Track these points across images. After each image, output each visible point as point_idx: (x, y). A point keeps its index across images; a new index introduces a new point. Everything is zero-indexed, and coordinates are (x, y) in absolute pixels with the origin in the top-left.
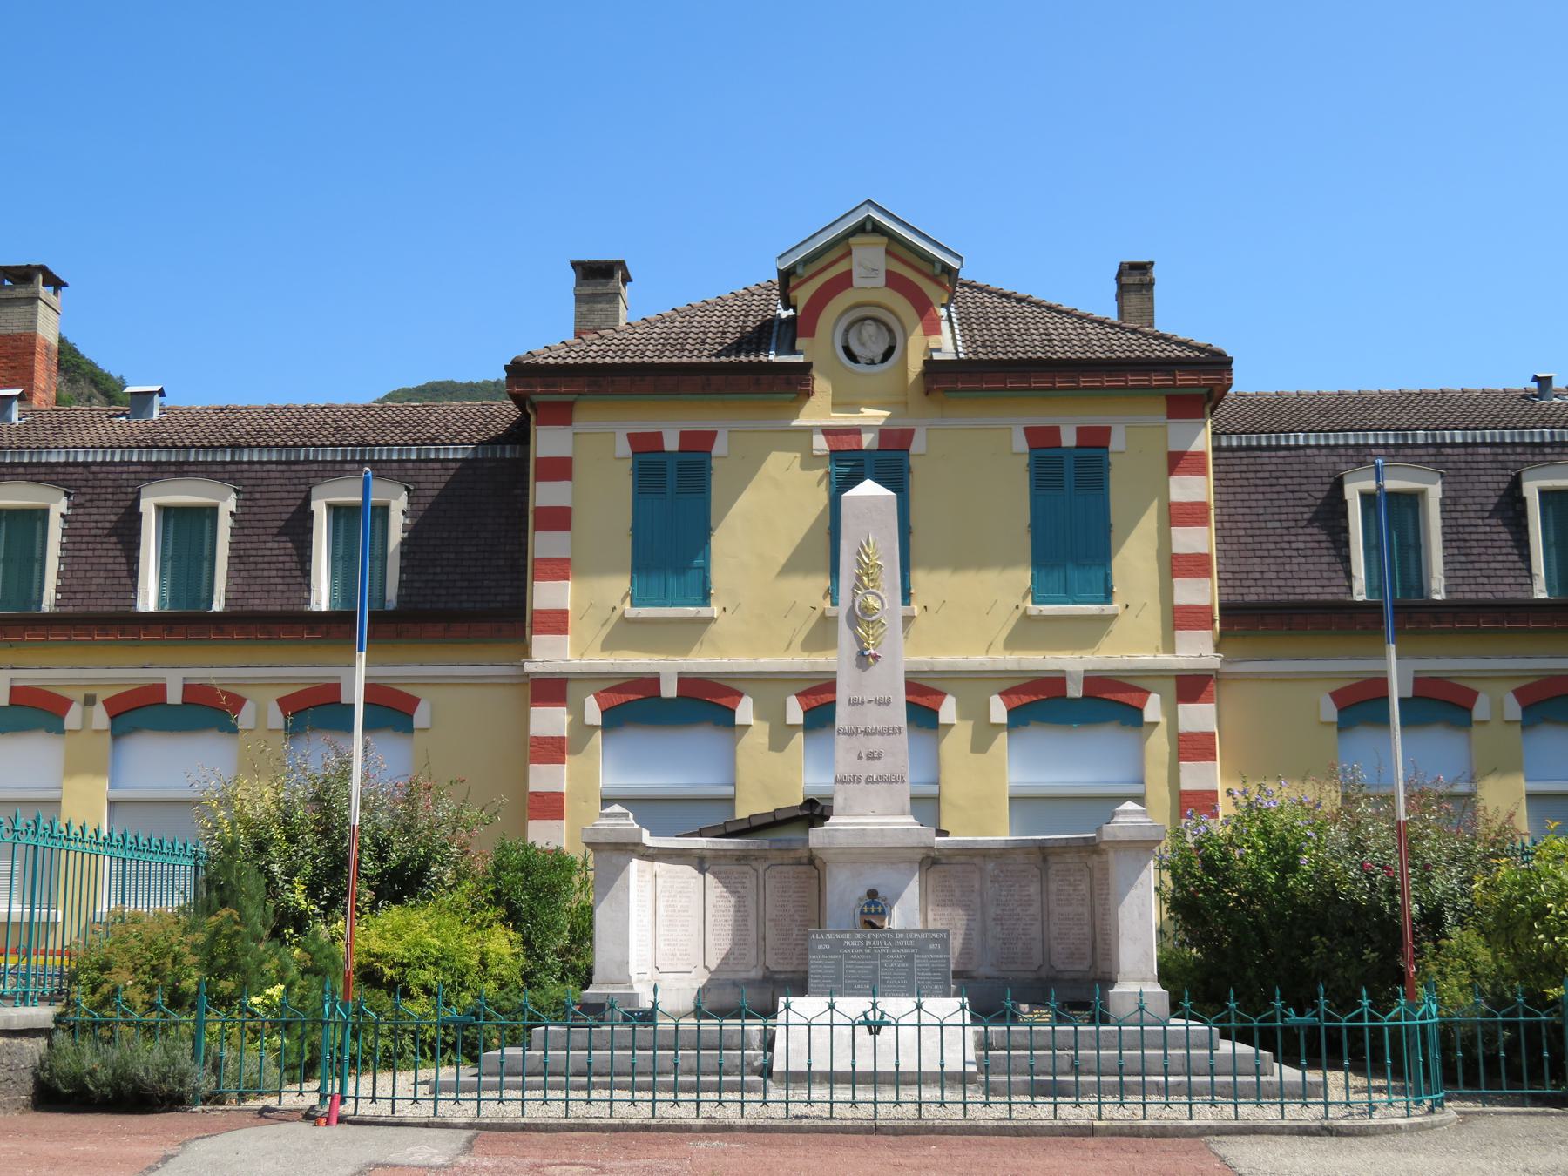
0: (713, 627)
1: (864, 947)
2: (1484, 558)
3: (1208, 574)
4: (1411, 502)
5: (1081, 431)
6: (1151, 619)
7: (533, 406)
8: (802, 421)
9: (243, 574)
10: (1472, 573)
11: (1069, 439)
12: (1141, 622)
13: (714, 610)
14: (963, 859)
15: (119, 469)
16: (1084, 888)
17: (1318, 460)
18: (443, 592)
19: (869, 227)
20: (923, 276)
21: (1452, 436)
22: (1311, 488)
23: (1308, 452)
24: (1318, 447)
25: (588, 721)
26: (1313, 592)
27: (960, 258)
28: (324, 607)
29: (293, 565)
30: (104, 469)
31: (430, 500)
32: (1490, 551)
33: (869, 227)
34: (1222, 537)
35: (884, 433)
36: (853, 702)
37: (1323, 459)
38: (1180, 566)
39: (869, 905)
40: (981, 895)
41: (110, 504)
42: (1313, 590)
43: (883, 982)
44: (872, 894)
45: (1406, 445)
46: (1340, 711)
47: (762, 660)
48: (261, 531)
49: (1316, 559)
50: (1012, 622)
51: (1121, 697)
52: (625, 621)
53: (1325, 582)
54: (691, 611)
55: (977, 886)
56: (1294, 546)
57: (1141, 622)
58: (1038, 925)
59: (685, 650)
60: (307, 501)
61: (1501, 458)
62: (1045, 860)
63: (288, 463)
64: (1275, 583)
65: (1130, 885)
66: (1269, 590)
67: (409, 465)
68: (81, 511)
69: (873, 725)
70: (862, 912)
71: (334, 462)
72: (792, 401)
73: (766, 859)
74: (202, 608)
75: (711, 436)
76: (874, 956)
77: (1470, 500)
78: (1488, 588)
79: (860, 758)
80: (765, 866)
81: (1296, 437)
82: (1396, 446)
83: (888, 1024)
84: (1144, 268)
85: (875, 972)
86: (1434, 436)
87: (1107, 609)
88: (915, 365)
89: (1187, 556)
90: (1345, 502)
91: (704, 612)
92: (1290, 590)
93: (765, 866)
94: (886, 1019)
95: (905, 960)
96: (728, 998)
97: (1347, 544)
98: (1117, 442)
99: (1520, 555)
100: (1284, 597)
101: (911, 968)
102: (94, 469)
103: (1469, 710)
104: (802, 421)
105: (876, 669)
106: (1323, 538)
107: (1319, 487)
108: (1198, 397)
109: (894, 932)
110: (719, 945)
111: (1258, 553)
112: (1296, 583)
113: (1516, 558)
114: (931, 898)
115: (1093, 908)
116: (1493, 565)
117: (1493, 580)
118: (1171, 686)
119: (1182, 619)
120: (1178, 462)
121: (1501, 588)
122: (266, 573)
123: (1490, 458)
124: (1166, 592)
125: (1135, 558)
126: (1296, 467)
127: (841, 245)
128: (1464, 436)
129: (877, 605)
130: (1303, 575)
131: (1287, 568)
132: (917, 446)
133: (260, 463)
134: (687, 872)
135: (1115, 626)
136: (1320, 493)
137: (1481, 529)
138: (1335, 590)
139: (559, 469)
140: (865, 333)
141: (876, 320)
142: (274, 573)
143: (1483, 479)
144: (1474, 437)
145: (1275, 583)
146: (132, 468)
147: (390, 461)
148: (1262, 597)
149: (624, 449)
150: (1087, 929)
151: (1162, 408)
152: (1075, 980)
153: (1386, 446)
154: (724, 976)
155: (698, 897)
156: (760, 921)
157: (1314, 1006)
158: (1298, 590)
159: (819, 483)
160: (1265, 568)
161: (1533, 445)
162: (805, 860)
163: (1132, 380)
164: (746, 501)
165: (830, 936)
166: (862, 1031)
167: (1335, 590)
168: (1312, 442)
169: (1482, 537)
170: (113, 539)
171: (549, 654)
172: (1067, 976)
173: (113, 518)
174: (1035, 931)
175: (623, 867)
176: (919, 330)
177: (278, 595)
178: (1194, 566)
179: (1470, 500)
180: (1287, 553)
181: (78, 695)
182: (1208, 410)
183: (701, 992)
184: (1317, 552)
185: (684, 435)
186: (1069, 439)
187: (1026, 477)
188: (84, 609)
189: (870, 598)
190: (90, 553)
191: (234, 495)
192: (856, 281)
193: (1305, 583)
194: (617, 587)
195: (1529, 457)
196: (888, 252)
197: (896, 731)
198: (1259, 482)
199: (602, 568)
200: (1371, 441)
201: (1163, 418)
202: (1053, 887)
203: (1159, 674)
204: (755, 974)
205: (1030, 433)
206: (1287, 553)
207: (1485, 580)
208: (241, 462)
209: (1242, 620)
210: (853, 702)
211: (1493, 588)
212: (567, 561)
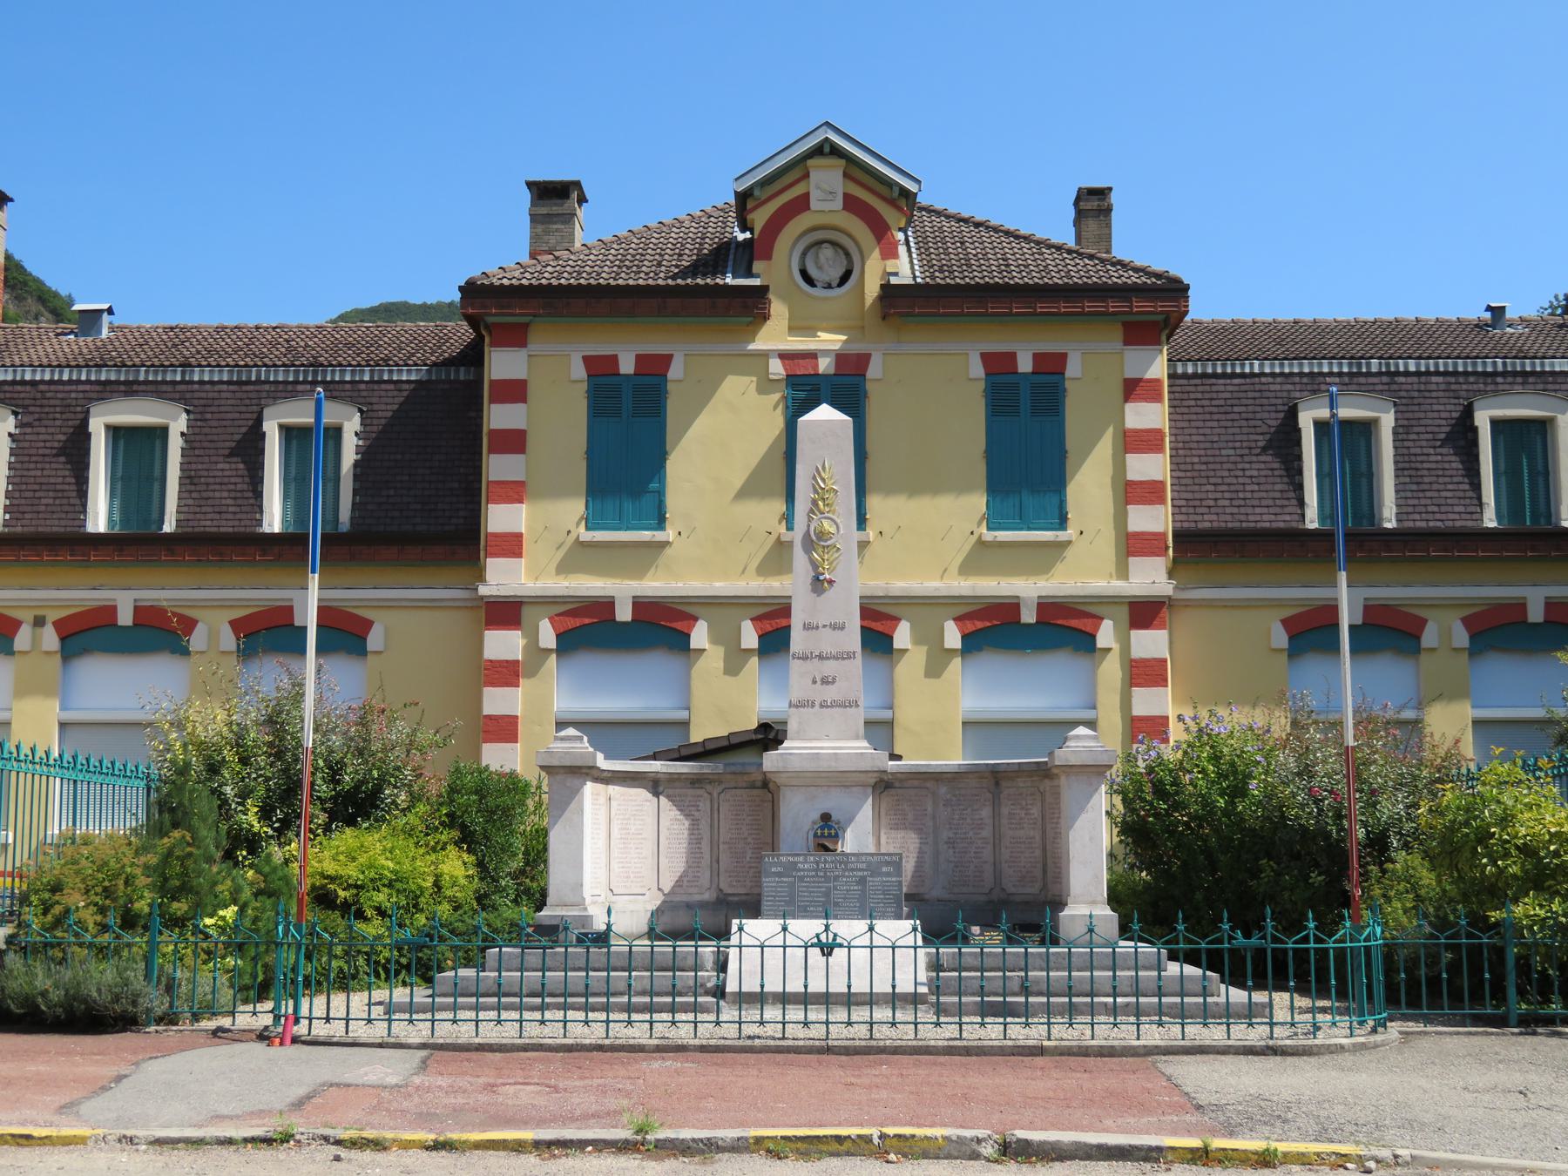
0: (668, 551)
1: (816, 870)
2: (1435, 487)
3: (1162, 501)
4: (1366, 429)
5: (1038, 358)
6: (1105, 545)
7: (487, 327)
8: (758, 345)
9: (194, 495)
10: (1423, 502)
11: (1025, 364)
12: (1091, 551)
13: (669, 534)
14: (916, 783)
15: (67, 388)
16: (1035, 812)
17: (1272, 387)
18: (397, 514)
19: (827, 149)
20: (881, 200)
21: (1406, 365)
22: (1266, 415)
23: (1263, 380)
24: (1273, 375)
25: (542, 645)
26: (1265, 519)
27: (918, 182)
28: (277, 529)
29: (245, 487)
30: (53, 388)
31: (383, 421)
32: (1441, 480)
33: (827, 149)
34: (1176, 465)
35: (841, 358)
36: (808, 627)
37: (1278, 387)
38: (1135, 493)
39: (822, 828)
40: (934, 818)
41: (58, 423)
42: (1265, 517)
43: (837, 904)
44: (826, 817)
45: (1359, 374)
46: (1291, 638)
47: (717, 584)
48: (212, 452)
49: (1269, 487)
50: (968, 547)
51: (1074, 623)
52: (579, 544)
53: (1278, 510)
54: (646, 535)
55: (930, 809)
56: (1248, 473)
57: (1091, 551)
58: (990, 847)
59: (640, 573)
60: (259, 421)
61: (1453, 387)
62: (997, 784)
63: (239, 383)
64: (1228, 510)
65: (1082, 809)
66: (1222, 518)
67: (363, 386)
68: (29, 430)
69: (828, 649)
70: (815, 835)
71: (286, 383)
73: (720, 782)
74: (153, 528)
75: (666, 360)
76: (827, 879)
77: (1422, 429)
78: (1438, 516)
79: (814, 682)
80: (720, 789)
81: (1252, 365)
82: (1350, 374)
83: (841, 946)
84: (1102, 193)
85: (827, 894)
86: (1388, 365)
87: (1062, 536)
88: (872, 290)
89: (1141, 483)
90: (1299, 430)
91: (659, 536)
92: (1243, 518)
93: (720, 789)
94: (839, 940)
95: (858, 883)
96: (682, 920)
97: (1300, 472)
98: (1073, 369)
99: (1471, 484)
100: (1237, 525)
101: (864, 891)
102: (42, 387)
103: (1418, 638)
104: (758, 345)
105: (831, 594)
106: (1276, 466)
107: (1273, 415)
108: (1155, 323)
109: (847, 855)
110: (673, 867)
111: (1212, 480)
112: (1250, 510)
113: (1467, 487)
114: (884, 821)
115: (1044, 832)
116: (1444, 494)
117: (1443, 509)
118: (1124, 613)
119: (1135, 545)
120: (1134, 389)
121: (1451, 516)
122: (217, 494)
123: (1443, 387)
124: (1121, 518)
125: (1089, 485)
126: (1250, 395)
127: (798, 167)
128: (1418, 365)
129: (833, 530)
130: (1256, 503)
131: (1241, 495)
132: (874, 371)
133: (211, 382)
134: (641, 795)
135: (1069, 553)
137: (1433, 458)
138: (1288, 518)
139: (514, 391)
140: (822, 258)
141: (834, 244)
142: (225, 494)
143: (1435, 407)
144: (1427, 366)
145: (1228, 510)
146: (81, 388)
147: (343, 382)
148: (1215, 525)
149: (579, 371)
150: (1038, 853)
151: (1118, 334)
152: (1027, 903)
153: (1340, 374)
154: (677, 899)
155: (652, 820)
156: (714, 844)
157: (1262, 929)
158: (1251, 518)
159: (775, 408)
160: (1219, 495)
161: (1485, 374)
162: (759, 784)
163: (1088, 306)
164: (702, 425)
165: (783, 859)
166: (815, 952)
167: (1288, 518)
168: (1267, 370)
169: (1433, 466)
170: (62, 459)
171: (503, 578)
172: (1018, 899)
173: (63, 438)
174: (987, 853)
175: (576, 791)
176: (876, 253)
177: (230, 516)
178: (1148, 493)
179: (1422, 429)
180: (1241, 480)
181: (26, 616)
182: (1164, 338)
183: (656, 914)
184: (1270, 480)
185: (639, 358)
186: (1025, 364)
187: (983, 402)
188: (32, 529)
189: (826, 524)
190: (39, 473)
191: (184, 416)
192: (814, 205)
193: (1258, 510)
194: (572, 510)
195: (1482, 386)
196: (846, 175)
197: (850, 656)
198: (1215, 410)
199: (557, 491)
200: (1326, 370)
201: (1119, 345)
202: (1005, 811)
203: (1112, 601)
204: (707, 896)
205: (987, 358)
206: (1241, 480)
207: (1436, 509)
208: (192, 382)
209: (1194, 547)
210: (808, 627)
211: (1443, 517)
212: (522, 484)
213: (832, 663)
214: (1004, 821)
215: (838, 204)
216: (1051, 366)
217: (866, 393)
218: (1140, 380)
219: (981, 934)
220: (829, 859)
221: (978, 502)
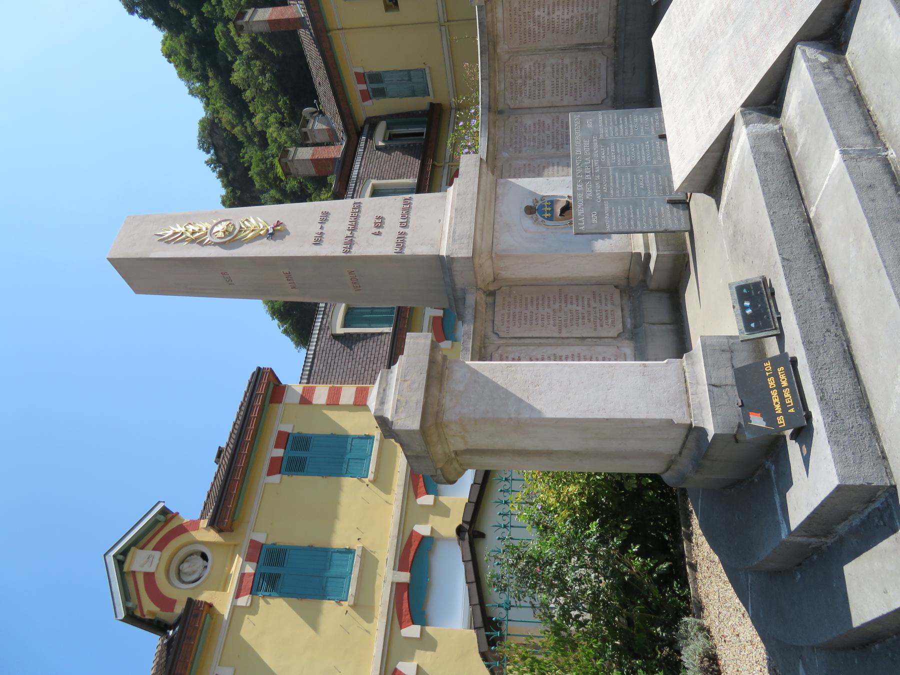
1: (593, 181)
19: (121, 557)
20: (162, 527)
24: (316, 346)
26: (386, 348)
27: (159, 502)
33: (121, 557)
35: (248, 559)
39: (542, 213)
44: (530, 210)
47: (375, 651)
50: (376, 489)
62: (501, 112)
70: (551, 219)
72: (212, 618)
73: (485, 337)
79: (379, 234)
80: (494, 337)
85: (622, 171)
88: (212, 536)
89: (356, 398)
97: (365, 334)
98: (287, 428)
120: (305, 400)
129: (224, 224)
132: (261, 538)
136: (338, 345)
151: (275, 405)
152: (616, 74)
153: (323, 318)
156: (562, 341)
159: (268, 603)
172: (611, 86)
176: (194, 533)
186: (280, 453)
192: (151, 570)
196: (142, 548)
201: (281, 405)
202: (526, 102)
205: (270, 473)
210: (318, 241)
213: (361, 222)
214: (536, 103)
215: (157, 554)
216: (283, 439)
217: (274, 544)
218: (302, 396)
221: (348, 483)
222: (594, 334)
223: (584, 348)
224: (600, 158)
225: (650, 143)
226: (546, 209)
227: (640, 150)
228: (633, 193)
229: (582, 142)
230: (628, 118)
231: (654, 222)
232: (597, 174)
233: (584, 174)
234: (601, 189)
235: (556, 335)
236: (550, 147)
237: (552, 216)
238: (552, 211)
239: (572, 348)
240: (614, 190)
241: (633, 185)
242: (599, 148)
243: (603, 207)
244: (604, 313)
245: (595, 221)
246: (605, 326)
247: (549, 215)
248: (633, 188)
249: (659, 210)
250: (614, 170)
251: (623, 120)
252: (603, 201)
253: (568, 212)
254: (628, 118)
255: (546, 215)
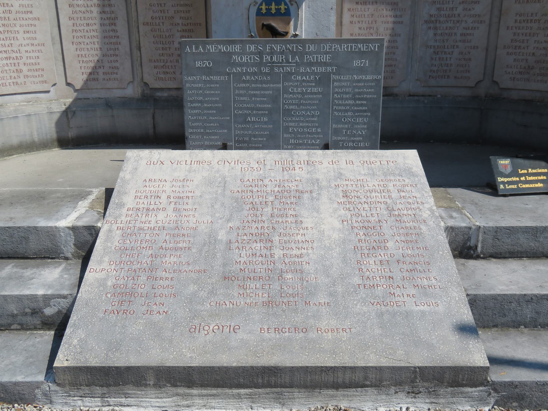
1: (260, 64)
43: (287, 113)
70: (259, 13)
85: (275, 99)
95: (319, 83)
96: (101, 122)
152: (528, 102)
156: (132, 26)
165: (212, 48)
183: (68, 113)
204: (132, 91)
219: (514, 173)
220: (277, 48)
222: (144, 60)
223: (128, 49)
224: (297, 73)
225: (318, 133)
226: (273, 7)
227: (307, 122)
228: (241, 109)
229: (326, 53)
230: (365, 111)
231: (197, 127)
232: (272, 68)
233: (272, 53)
234: (247, 73)
235: (141, 19)
236: (433, 12)
237: (262, 15)
238: (269, 13)
239: (126, 37)
240: (244, 88)
241: (252, 109)
242: (316, 74)
243: (220, 74)
244: (172, 70)
245: (198, 64)
246: (156, 71)
247: (264, 11)
248: (248, 109)
249: (215, 134)
250: (278, 90)
251: (362, 105)
252: (229, 74)
253: (269, 33)
254: (365, 111)
255: (264, 7)
